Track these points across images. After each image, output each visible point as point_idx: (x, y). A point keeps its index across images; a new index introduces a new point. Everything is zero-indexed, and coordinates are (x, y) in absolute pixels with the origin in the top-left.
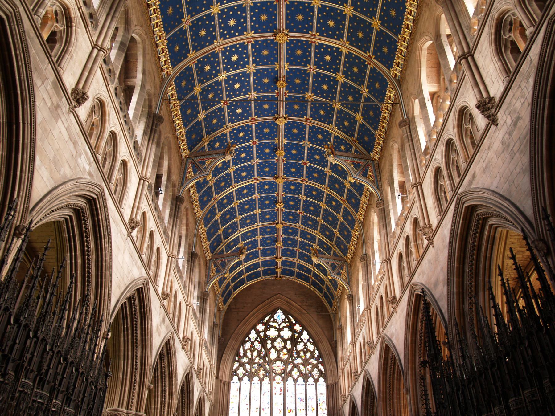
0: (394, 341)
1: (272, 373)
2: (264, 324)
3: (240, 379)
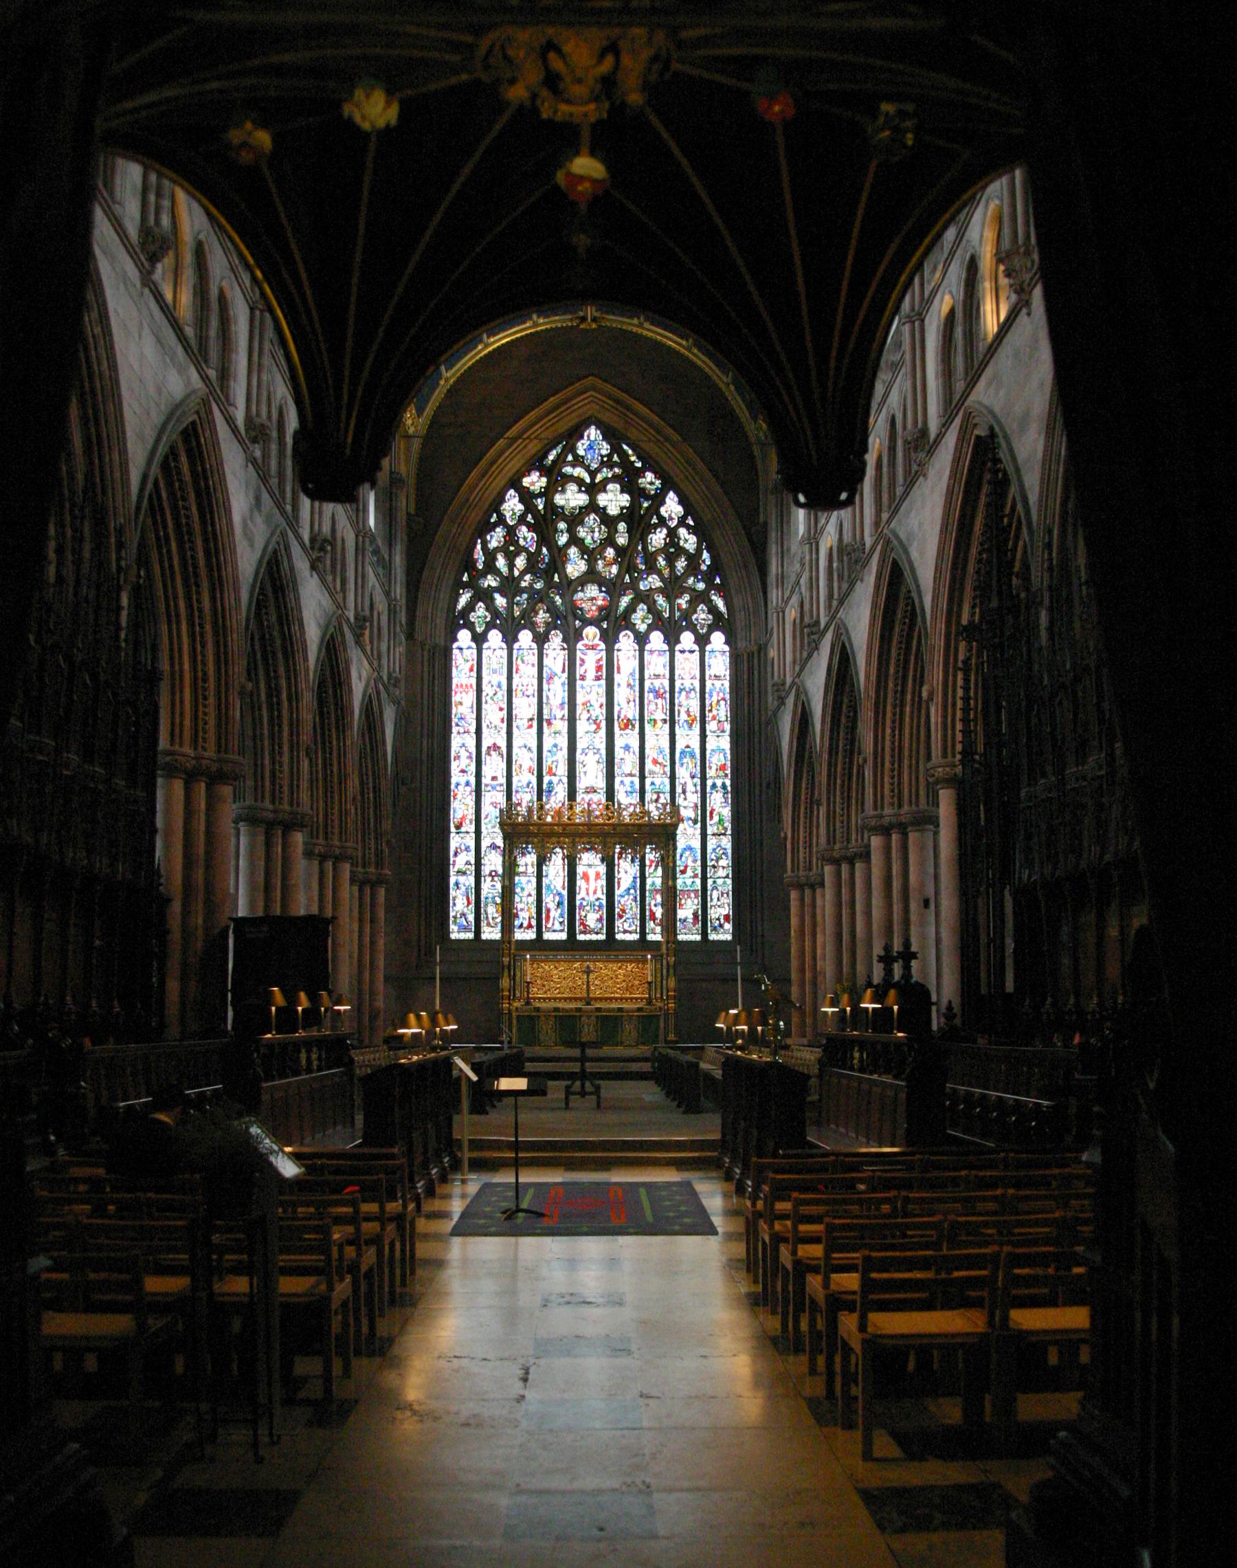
0: (914, 555)
1: (570, 618)
2: (545, 471)
3: (479, 639)
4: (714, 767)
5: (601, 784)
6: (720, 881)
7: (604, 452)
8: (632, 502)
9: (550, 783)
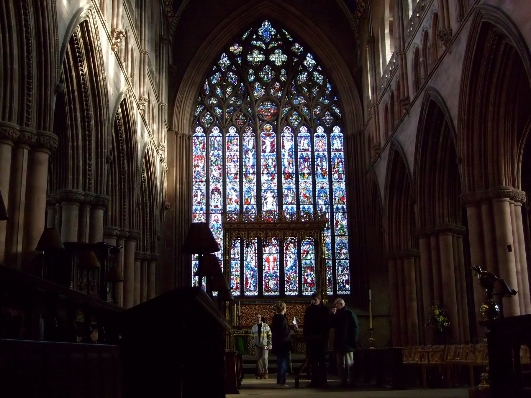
3: (207, 131)
4: (337, 198)
5: (275, 208)
6: (343, 261)
7: (273, 33)
8: (288, 59)
9: (247, 208)
